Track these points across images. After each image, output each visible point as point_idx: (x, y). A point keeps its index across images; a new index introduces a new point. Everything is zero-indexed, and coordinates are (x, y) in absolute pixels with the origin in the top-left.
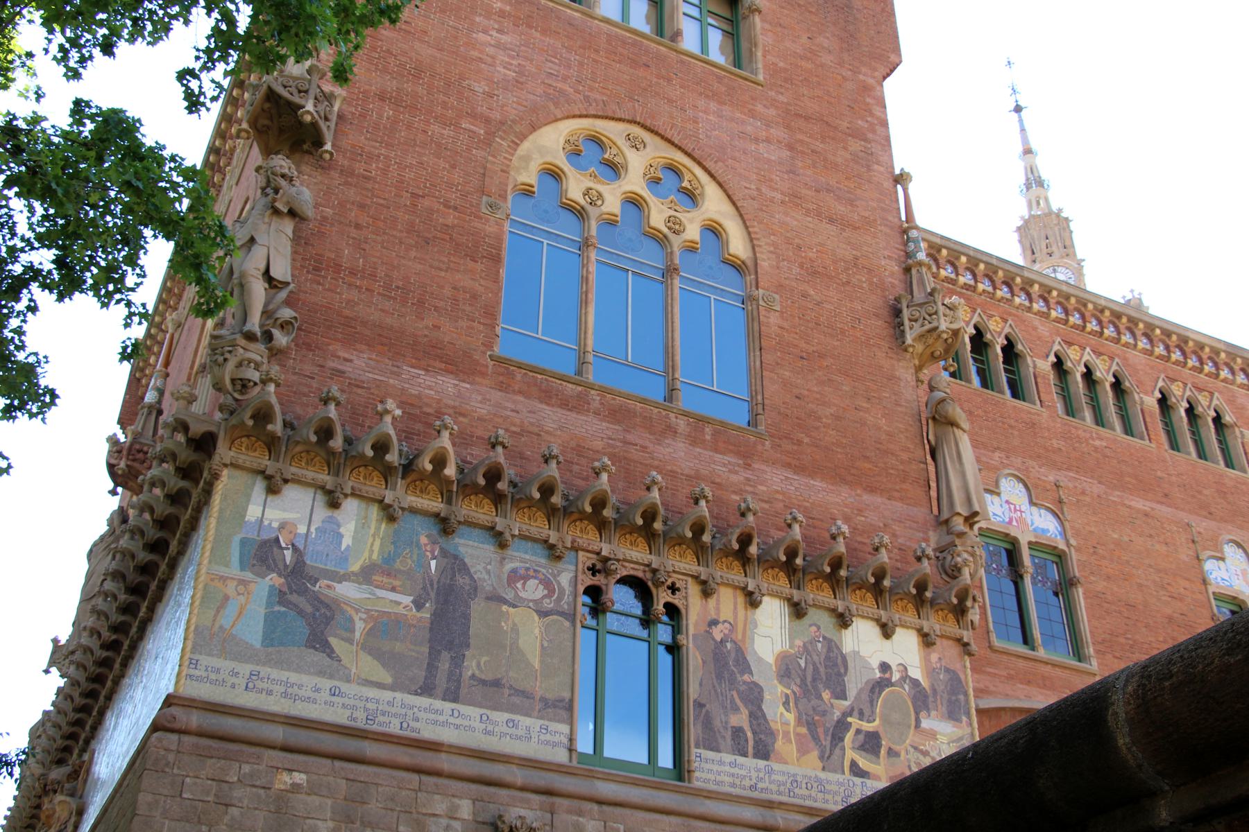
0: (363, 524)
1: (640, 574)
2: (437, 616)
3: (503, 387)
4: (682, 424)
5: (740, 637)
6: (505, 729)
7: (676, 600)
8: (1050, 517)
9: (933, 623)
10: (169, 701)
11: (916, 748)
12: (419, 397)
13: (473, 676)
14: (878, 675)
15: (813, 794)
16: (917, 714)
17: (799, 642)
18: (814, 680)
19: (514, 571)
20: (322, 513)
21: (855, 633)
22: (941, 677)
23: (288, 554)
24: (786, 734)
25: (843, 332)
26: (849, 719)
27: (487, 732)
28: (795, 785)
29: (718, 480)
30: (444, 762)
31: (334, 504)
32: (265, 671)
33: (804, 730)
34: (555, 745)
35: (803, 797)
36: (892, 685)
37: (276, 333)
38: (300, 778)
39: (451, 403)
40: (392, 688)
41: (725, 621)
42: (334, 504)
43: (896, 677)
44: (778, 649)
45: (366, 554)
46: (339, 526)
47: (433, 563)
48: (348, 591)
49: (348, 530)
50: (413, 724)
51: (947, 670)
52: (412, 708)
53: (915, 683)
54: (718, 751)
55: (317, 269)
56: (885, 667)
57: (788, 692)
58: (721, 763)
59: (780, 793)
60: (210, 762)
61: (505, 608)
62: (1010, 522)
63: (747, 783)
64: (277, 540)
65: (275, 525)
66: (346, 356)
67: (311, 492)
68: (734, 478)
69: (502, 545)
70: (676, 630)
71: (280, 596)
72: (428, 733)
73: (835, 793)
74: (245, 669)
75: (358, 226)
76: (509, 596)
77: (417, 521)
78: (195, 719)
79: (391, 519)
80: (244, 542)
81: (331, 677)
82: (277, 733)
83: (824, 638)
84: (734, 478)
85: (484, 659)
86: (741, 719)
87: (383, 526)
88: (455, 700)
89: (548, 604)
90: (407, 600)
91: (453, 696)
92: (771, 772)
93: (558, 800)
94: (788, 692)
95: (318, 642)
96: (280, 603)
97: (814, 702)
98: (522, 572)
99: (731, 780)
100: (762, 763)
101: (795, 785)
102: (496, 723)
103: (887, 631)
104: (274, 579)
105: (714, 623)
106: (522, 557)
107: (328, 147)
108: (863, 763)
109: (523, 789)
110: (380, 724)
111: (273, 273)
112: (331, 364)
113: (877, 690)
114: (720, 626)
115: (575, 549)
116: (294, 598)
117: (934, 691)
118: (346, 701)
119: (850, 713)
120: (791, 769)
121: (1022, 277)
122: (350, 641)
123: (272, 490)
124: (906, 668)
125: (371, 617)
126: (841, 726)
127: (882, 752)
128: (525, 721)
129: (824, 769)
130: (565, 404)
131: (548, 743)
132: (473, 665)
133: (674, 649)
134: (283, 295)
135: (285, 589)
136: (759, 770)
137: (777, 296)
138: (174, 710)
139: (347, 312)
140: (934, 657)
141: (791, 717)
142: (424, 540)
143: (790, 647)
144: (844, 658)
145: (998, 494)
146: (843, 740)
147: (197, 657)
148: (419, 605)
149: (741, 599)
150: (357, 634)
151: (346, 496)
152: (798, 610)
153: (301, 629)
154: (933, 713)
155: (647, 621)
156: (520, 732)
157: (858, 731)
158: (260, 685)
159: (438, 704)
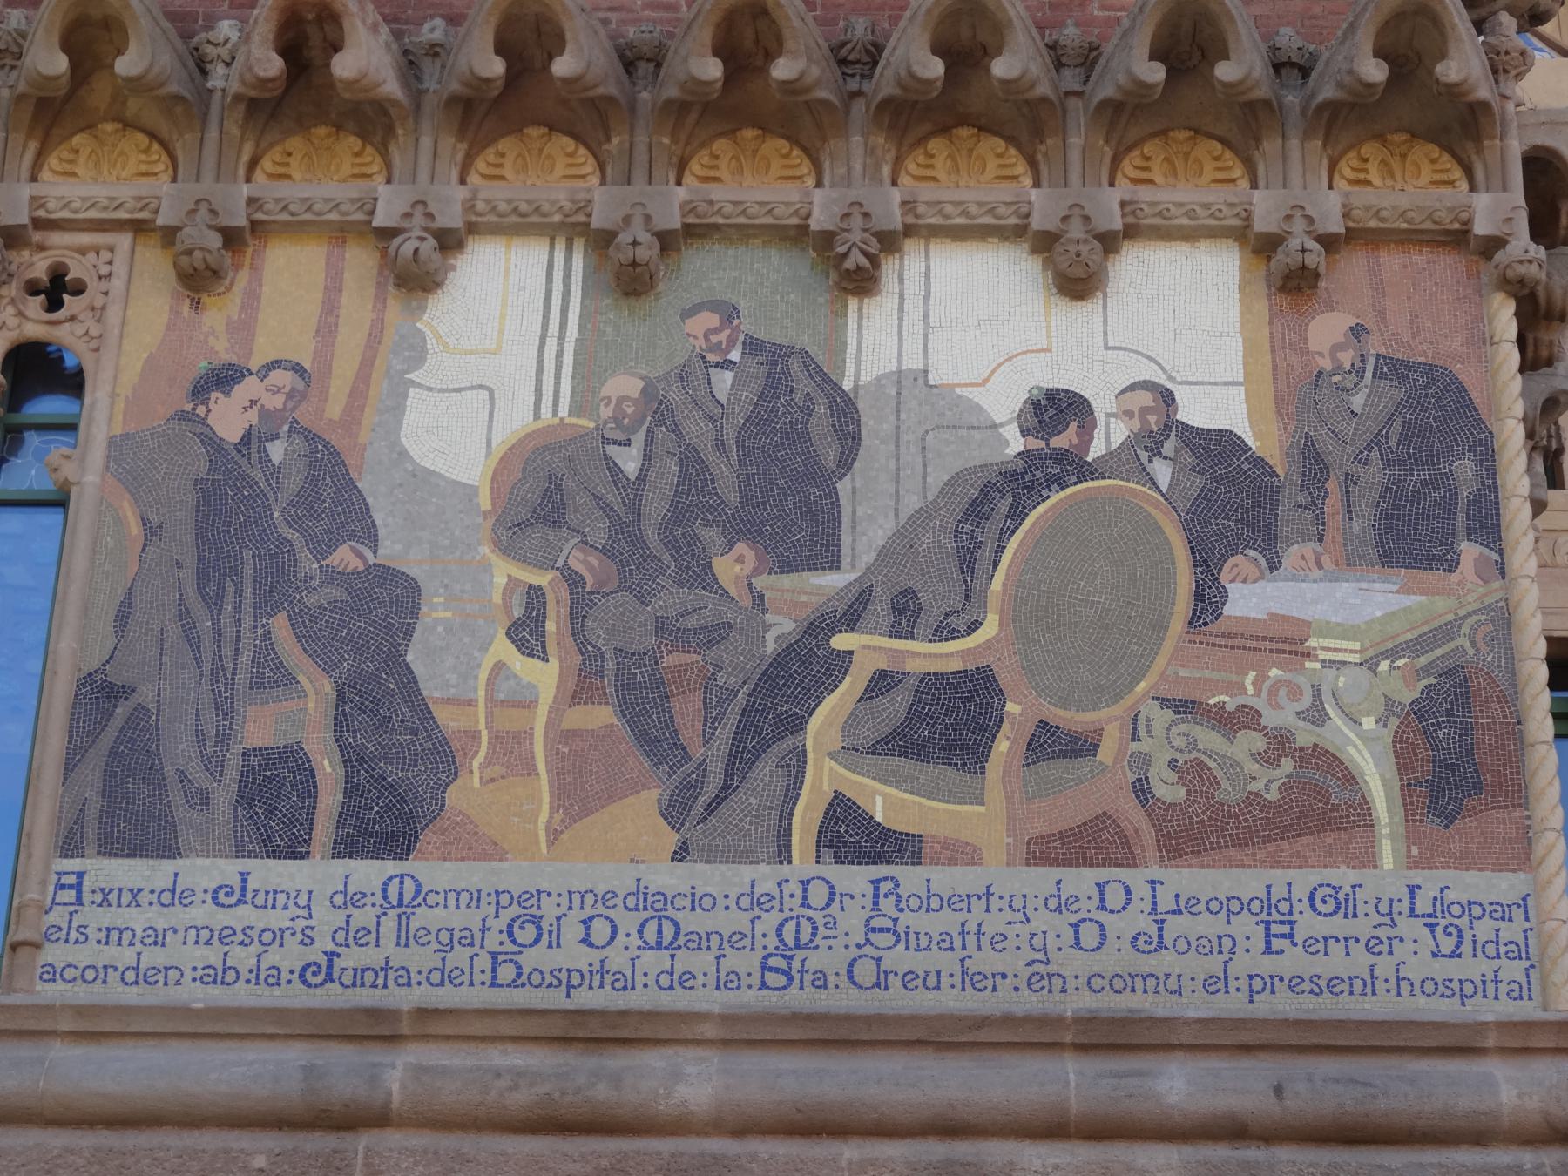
5: (335, 410)
15: (617, 959)
16: (1207, 565)
17: (624, 386)
18: (680, 514)
21: (913, 312)
22: (1358, 401)
26: (841, 641)
28: (529, 933)
33: (602, 715)
35: (566, 980)
36: (1086, 471)
41: (275, 364)
43: (1109, 435)
54: (168, 850)
57: (542, 579)
58: (176, 896)
59: (448, 978)
63: (289, 957)
73: (735, 940)
83: (753, 347)
94: (542, 579)
97: (670, 599)
99: (213, 955)
100: (368, 873)
101: (526, 935)
105: (224, 378)
113: (1005, 505)
114: (248, 388)
120: (513, 875)
124: (1167, 398)
127: (1002, 746)
129: (681, 854)
143: (577, 408)
144: (845, 410)
146: (797, 724)
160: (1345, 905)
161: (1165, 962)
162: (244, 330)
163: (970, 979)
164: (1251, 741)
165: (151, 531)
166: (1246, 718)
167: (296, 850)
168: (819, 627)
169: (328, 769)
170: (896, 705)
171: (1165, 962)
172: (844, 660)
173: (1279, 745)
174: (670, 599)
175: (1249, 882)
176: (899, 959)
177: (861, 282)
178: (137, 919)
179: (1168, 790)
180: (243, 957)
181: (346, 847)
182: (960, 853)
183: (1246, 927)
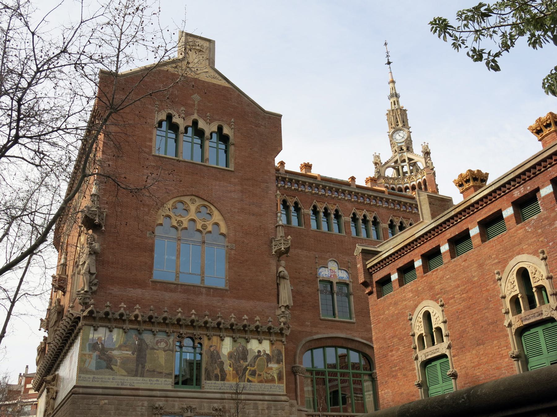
0: (118, 334)
1: (191, 336)
2: (138, 356)
3: (154, 289)
4: (204, 290)
6: (156, 382)
7: (202, 342)
8: (345, 272)
9: (274, 338)
10: (75, 387)
11: (266, 373)
12: (132, 297)
13: (148, 370)
14: (257, 354)
16: (267, 363)
17: (235, 348)
18: (238, 358)
19: (157, 341)
20: (108, 333)
23: (100, 346)
24: (230, 373)
25: (254, 251)
27: (151, 384)
29: (214, 305)
30: (141, 393)
31: (111, 331)
32: (96, 376)
33: (235, 372)
34: (168, 384)
36: (261, 356)
37: (93, 287)
38: (106, 401)
39: (140, 296)
40: (128, 376)
42: (111, 331)
43: (262, 354)
44: (229, 350)
45: (119, 343)
46: (112, 336)
47: (137, 342)
48: (115, 353)
49: (115, 337)
50: (133, 384)
51: (278, 350)
52: (132, 380)
53: (268, 355)
55: (103, 264)
56: (259, 352)
58: (212, 383)
60: (85, 400)
61: (155, 351)
62: (331, 276)
63: (218, 388)
64: (97, 342)
65: (97, 338)
66: (112, 288)
67: (104, 329)
68: (219, 304)
69: (154, 335)
70: (201, 350)
71: (99, 357)
72: (136, 386)
74: (92, 376)
75: (113, 249)
76: (156, 347)
77: (132, 331)
78: (81, 390)
79: (125, 332)
80: (89, 344)
81: (113, 375)
82: (100, 391)
84: (219, 304)
85: (150, 365)
86: (217, 371)
87: (124, 334)
88: (143, 377)
89: (167, 348)
90: (130, 353)
91: (142, 375)
92: (225, 384)
93: (168, 399)
95: (109, 367)
96: (99, 359)
98: (160, 340)
100: (222, 382)
102: (153, 381)
103: (260, 342)
104: (97, 353)
105: (211, 346)
106: (161, 336)
107: (103, 228)
108: (250, 378)
109: (160, 397)
110: (125, 385)
111: (91, 272)
112: (108, 292)
115: (173, 332)
116: (102, 357)
117: (273, 356)
118: (116, 380)
119: (248, 365)
120: (230, 383)
121: (341, 189)
122: (116, 365)
123: (95, 330)
125: (122, 359)
126: (246, 369)
128: (160, 379)
130: (171, 291)
131: (166, 384)
132: (147, 368)
133: (201, 354)
134: (94, 276)
135: (100, 355)
136: (222, 384)
137: (234, 245)
138: (75, 389)
139: (111, 275)
140: (274, 347)
141: (231, 369)
142: (134, 336)
145: (327, 268)
147: (80, 375)
148: (133, 354)
149: (219, 338)
150: (118, 363)
151: (113, 328)
152: (235, 340)
153: (104, 364)
154: (272, 362)
155: (194, 348)
156: (160, 382)
157: (250, 370)
158: (95, 380)
159: (139, 378)
160: (274, 386)
161: (265, 389)
162: (212, 343)
163: (255, 390)
164: (270, 375)
165: (208, 357)
166: (269, 374)
167: (218, 381)
168: (246, 367)
169: (219, 375)
170: (251, 372)
171: (265, 389)
172: (248, 369)
173: (271, 376)
174: (238, 364)
175: (269, 384)
176: (251, 389)
177: (248, 342)
178: (210, 385)
179: (265, 378)
180: (216, 388)
181: (221, 380)
182: (254, 382)
183: (269, 387)
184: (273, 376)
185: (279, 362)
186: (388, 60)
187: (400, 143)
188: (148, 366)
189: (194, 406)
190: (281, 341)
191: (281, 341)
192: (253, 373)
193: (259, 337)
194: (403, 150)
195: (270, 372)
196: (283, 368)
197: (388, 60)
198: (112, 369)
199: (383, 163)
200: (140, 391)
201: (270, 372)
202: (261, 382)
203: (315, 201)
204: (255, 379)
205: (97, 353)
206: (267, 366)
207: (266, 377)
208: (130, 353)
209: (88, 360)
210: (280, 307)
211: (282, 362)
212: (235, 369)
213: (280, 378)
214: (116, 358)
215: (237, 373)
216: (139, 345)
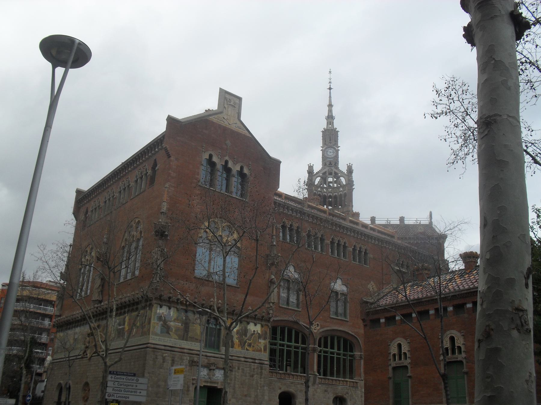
0: (174, 312)
9: (263, 323)
11: (257, 345)
17: (240, 328)
20: (168, 310)
24: (236, 344)
27: (191, 346)
31: (170, 309)
32: (161, 338)
33: (239, 343)
40: (179, 339)
42: (170, 309)
48: (172, 324)
49: (172, 313)
56: (254, 331)
74: (158, 337)
76: (195, 322)
82: (163, 347)
88: (187, 341)
90: (180, 324)
91: (187, 340)
95: (168, 332)
100: (232, 349)
103: (255, 325)
104: (161, 323)
108: (248, 348)
117: (262, 335)
122: (172, 332)
123: (161, 307)
126: (246, 342)
141: (237, 341)
148: (182, 325)
156: (196, 345)
159: (185, 342)
166: (259, 346)
173: (260, 347)
182: (250, 351)
184: (261, 348)
185: (265, 339)
186: (330, 86)
187: (330, 158)
188: (190, 334)
189: (216, 363)
190: (268, 325)
191: (268, 325)
192: (250, 345)
193: (255, 322)
194: (332, 164)
195: (259, 345)
196: (267, 343)
197: (330, 86)
198: (169, 334)
199: (315, 173)
200: (185, 350)
201: (259, 345)
202: (254, 351)
203: (285, 219)
204: (251, 349)
205: (161, 323)
206: (258, 341)
207: (257, 348)
208: (180, 324)
209: (156, 327)
210: (269, 303)
211: (267, 339)
212: (240, 341)
213: (265, 350)
214: (172, 327)
215: (241, 344)
216: (185, 319)
